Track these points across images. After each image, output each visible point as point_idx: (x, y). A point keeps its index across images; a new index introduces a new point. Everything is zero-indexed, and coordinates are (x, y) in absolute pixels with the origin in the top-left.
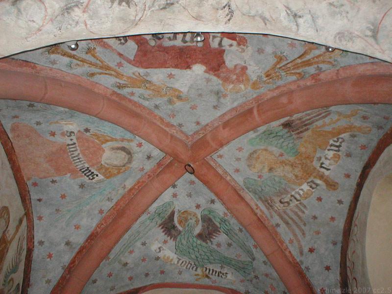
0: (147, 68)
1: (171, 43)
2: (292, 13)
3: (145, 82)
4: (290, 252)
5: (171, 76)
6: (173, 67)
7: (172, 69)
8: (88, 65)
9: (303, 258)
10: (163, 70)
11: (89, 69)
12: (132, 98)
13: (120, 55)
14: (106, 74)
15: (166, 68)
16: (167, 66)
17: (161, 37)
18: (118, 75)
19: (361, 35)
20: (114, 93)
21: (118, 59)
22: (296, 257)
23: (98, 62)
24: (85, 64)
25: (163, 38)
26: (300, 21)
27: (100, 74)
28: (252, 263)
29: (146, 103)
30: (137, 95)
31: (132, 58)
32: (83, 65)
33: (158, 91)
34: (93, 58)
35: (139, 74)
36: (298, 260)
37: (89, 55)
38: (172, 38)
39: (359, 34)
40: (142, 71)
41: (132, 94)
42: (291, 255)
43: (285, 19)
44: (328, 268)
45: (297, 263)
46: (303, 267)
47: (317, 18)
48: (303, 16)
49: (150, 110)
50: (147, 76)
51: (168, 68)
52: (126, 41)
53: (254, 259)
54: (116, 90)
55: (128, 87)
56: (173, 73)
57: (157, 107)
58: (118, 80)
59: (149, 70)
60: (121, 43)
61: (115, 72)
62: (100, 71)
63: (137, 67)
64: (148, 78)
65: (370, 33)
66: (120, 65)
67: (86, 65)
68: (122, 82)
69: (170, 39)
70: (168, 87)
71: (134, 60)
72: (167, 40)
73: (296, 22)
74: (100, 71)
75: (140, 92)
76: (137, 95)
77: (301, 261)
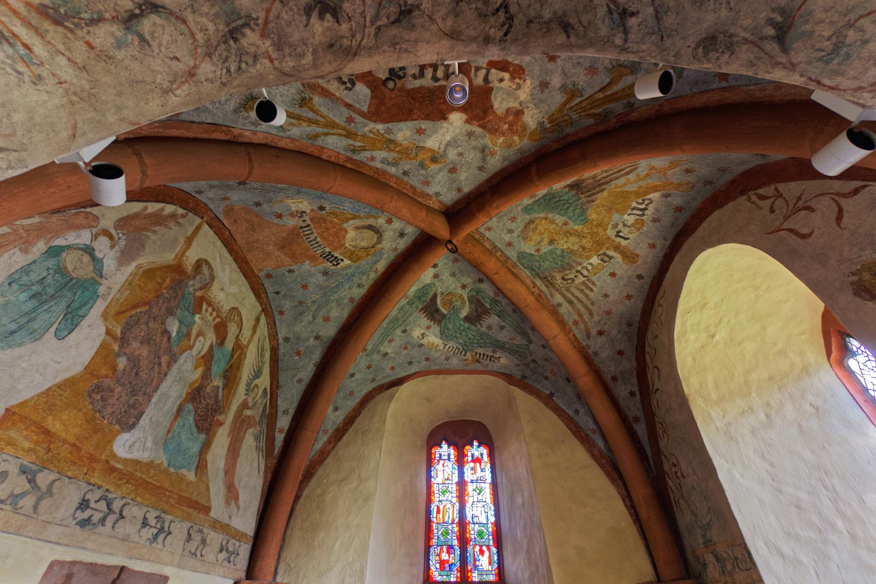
0: (387, 123)
1: (418, 83)
2: (618, 9)
3: (390, 144)
4: (574, 335)
5: (420, 131)
6: (422, 119)
7: (422, 121)
8: (306, 124)
9: (590, 342)
10: (410, 124)
11: (309, 129)
12: (373, 164)
13: (349, 106)
14: (333, 134)
15: (413, 120)
16: (415, 117)
17: (402, 75)
18: (349, 135)
19: (751, 38)
20: (349, 159)
21: (346, 113)
22: (581, 341)
23: (318, 118)
24: (301, 122)
25: (405, 76)
26: (632, 22)
27: (326, 134)
28: (528, 346)
29: (393, 170)
30: (379, 159)
31: (365, 109)
32: (300, 124)
33: (405, 153)
34: (311, 113)
35: (378, 131)
36: (584, 344)
37: (305, 109)
38: (417, 74)
39: (747, 35)
40: (380, 127)
41: (373, 159)
42: (576, 339)
43: (603, 22)
44: (621, 353)
45: (583, 347)
46: (590, 352)
47: (666, 12)
48: (638, 13)
49: (397, 178)
50: (389, 134)
51: (415, 120)
52: (353, 84)
53: (531, 342)
54: (349, 154)
55: (365, 150)
56: (423, 127)
57: (405, 173)
58: (351, 142)
59: (390, 125)
60: (346, 88)
61: (344, 130)
62: (325, 130)
63: (374, 122)
64: (391, 137)
65: (771, 31)
66: (350, 120)
67: (305, 124)
68: (358, 144)
69: (414, 77)
70: (418, 147)
71: (369, 112)
72: (410, 78)
73: (624, 25)
74: (325, 130)
75: (382, 156)
76: (379, 159)
77: (588, 345)
